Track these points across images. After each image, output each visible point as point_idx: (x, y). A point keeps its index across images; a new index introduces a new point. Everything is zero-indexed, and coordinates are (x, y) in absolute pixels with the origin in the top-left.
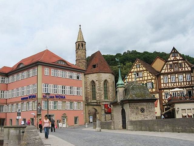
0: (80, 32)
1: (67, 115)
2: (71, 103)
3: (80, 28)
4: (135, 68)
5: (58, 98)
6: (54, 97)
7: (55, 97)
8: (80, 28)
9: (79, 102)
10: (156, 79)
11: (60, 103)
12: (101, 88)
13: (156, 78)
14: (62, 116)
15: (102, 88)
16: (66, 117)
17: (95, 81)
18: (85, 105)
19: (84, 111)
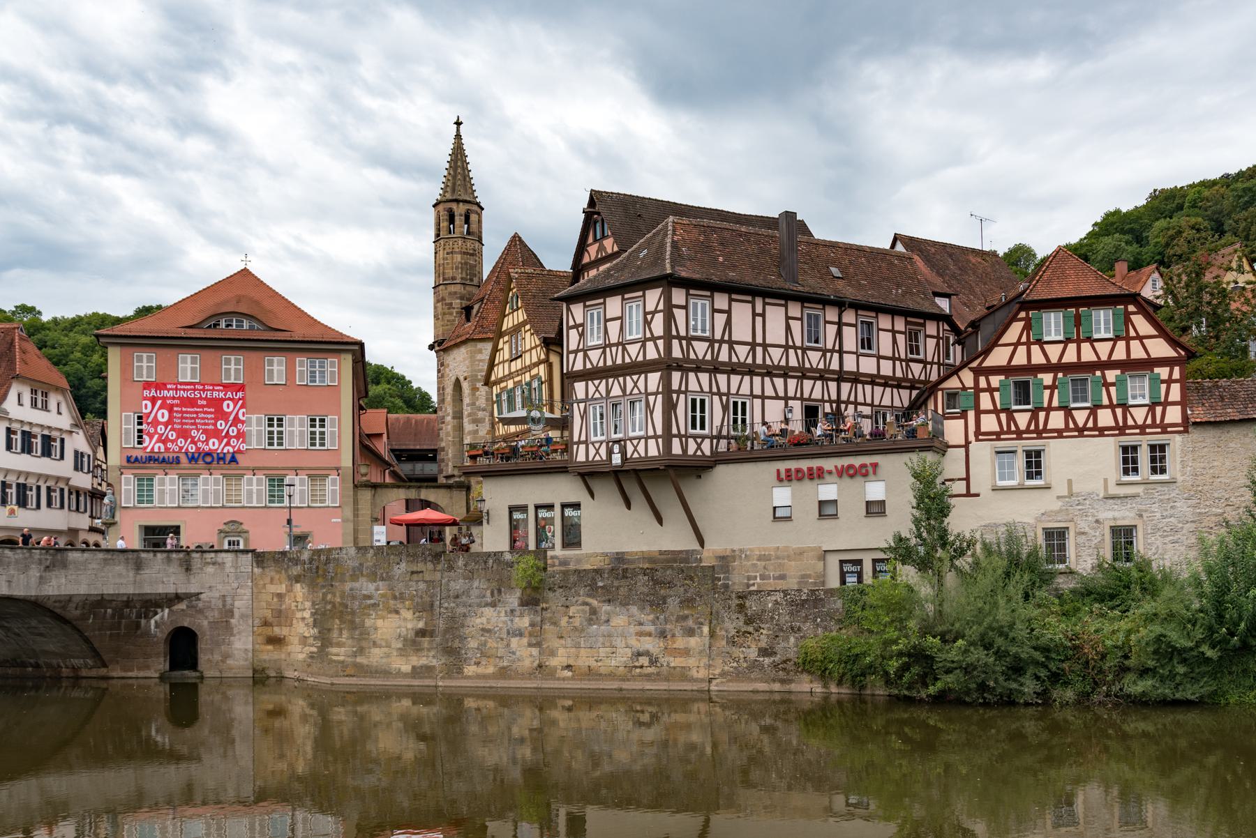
0: (458, 156)
1: (245, 527)
2: (277, 483)
3: (458, 136)
4: (508, 315)
5: (200, 462)
6: (178, 461)
7: (184, 459)
8: (458, 136)
9: (317, 476)
10: (547, 361)
11: (209, 486)
12: (480, 409)
13: (547, 355)
14: (221, 531)
15: (484, 410)
16: (244, 535)
17: (461, 379)
18: (355, 486)
19: (349, 513)
